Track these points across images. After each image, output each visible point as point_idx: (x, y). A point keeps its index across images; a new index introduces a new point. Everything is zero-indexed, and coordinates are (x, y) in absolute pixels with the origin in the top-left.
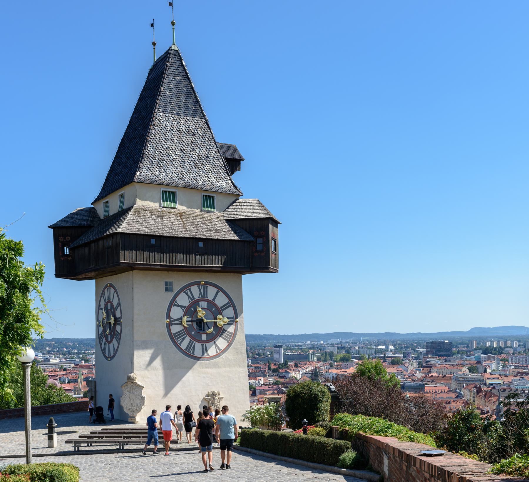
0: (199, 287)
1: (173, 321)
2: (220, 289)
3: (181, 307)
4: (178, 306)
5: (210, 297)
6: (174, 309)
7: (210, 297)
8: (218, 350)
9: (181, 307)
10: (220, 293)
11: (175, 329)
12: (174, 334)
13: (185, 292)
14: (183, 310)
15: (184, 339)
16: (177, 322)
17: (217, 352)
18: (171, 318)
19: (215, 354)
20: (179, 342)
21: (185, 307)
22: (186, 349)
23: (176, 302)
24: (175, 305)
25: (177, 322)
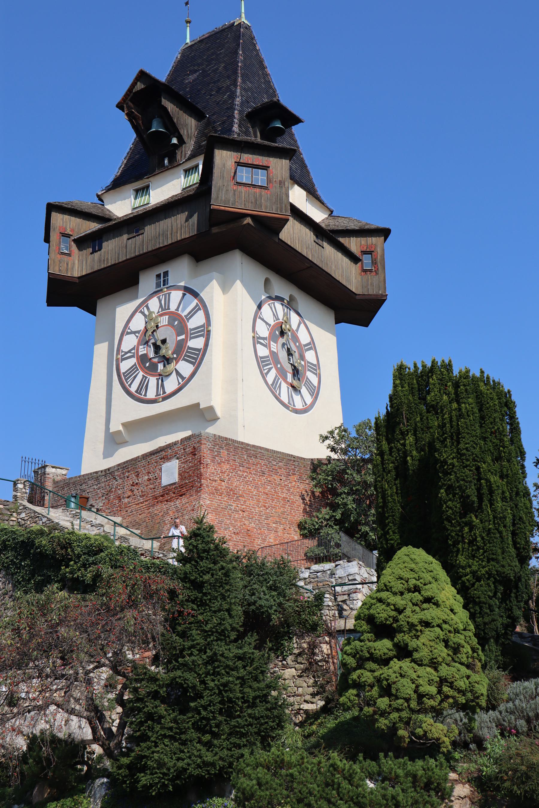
3: (267, 323)
4: (263, 320)
6: (258, 321)
9: (267, 323)
10: (302, 325)
12: (261, 358)
13: (269, 305)
15: (270, 369)
16: (262, 341)
20: (266, 371)
21: (270, 325)
22: (272, 385)
24: (260, 318)
25: (262, 341)
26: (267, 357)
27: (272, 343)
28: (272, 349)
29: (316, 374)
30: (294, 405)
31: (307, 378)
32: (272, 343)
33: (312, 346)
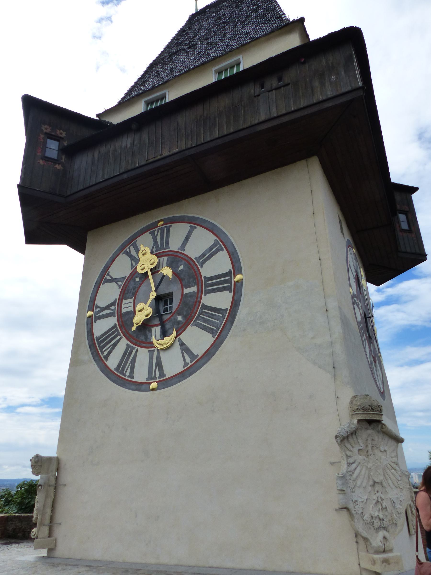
0: (152, 233)
1: (100, 312)
2: (194, 222)
4: (112, 280)
5: (174, 245)
6: (104, 288)
7: (174, 245)
8: (188, 359)
10: (199, 231)
11: (101, 328)
12: (98, 338)
14: (120, 286)
15: (115, 345)
16: (107, 312)
17: (186, 364)
18: (97, 307)
19: (180, 368)
20: (105, 353)
23: (108, 275)
25: (107, 312)
26: (115, 326)
27: (124, 301)
28: (123, 311)
29: (228, 289)
30: (162, 374)
31: (205, 307)
32: (124, 301)
33: (223, 243)
